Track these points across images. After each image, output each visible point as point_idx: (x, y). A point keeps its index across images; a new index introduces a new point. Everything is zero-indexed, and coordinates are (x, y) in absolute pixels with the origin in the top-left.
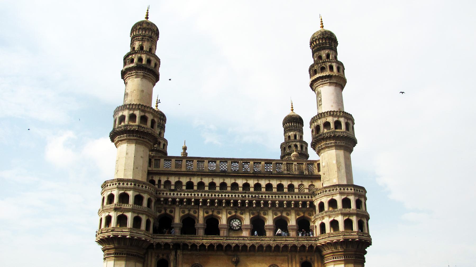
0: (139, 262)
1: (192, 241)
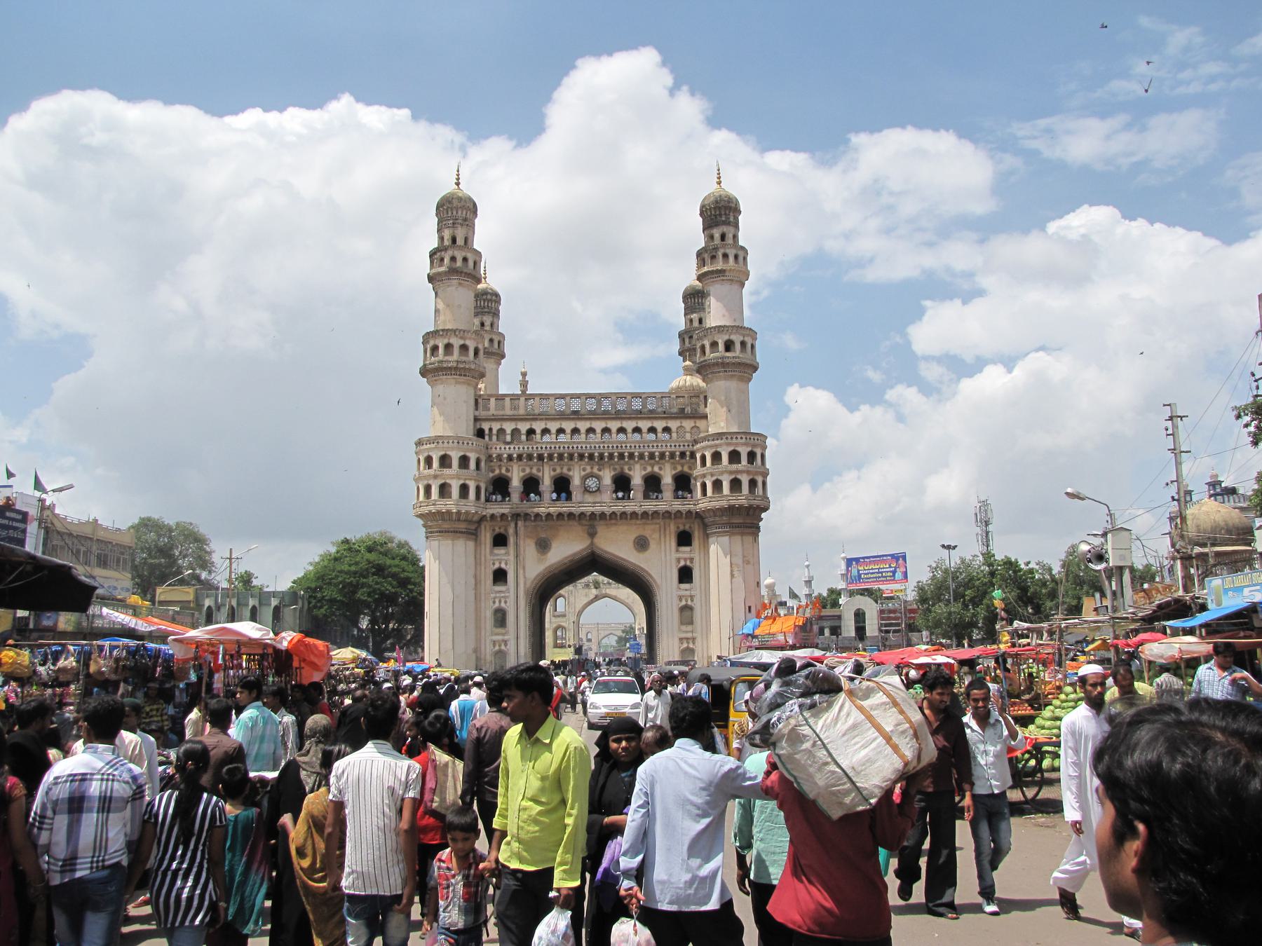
0: (469, 539)
1: (536, 510)
